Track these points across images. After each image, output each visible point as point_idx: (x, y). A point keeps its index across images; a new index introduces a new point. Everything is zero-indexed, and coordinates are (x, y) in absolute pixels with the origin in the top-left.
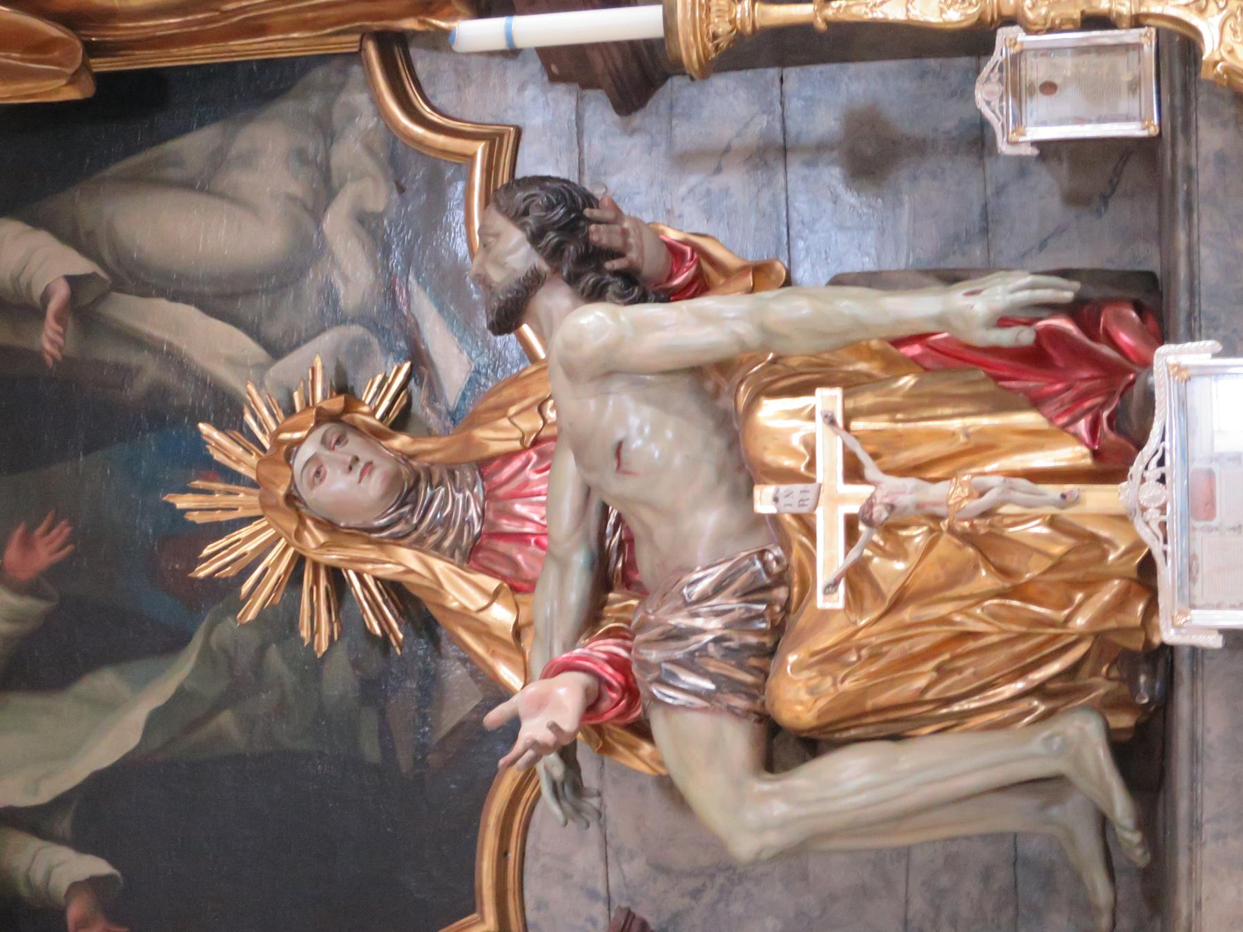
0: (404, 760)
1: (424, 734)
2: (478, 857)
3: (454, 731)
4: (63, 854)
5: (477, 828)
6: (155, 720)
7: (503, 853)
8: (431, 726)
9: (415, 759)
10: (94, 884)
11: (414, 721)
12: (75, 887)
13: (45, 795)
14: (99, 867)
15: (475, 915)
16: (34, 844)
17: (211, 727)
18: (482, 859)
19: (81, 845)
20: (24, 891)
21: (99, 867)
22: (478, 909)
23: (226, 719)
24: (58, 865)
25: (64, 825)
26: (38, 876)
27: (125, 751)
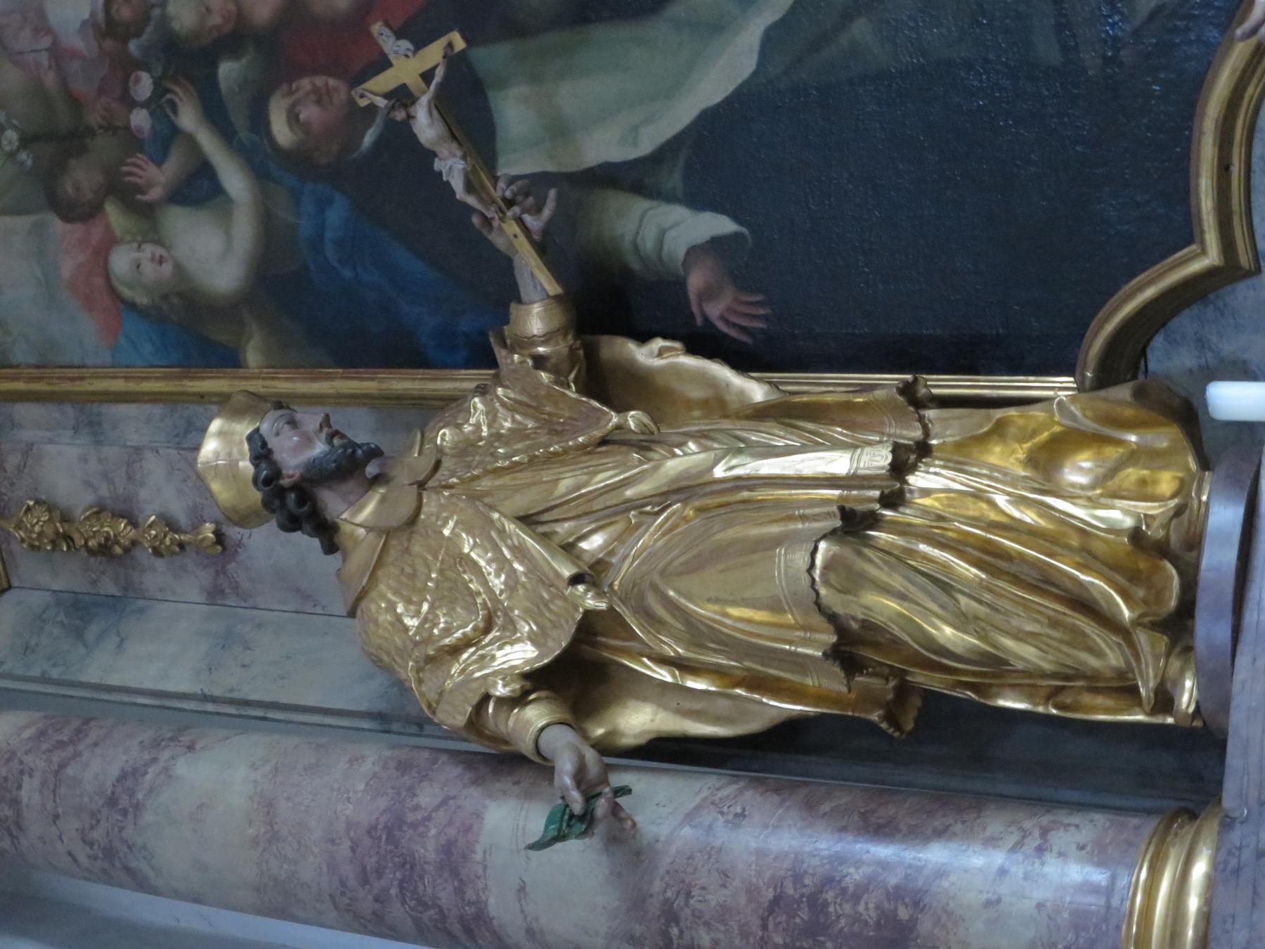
0: (1090, 58)
1: (1113, 26)
2: (1192, 170)
3: (1153, 16)
4: (676, 213)
5: (1189, 140)
6: (772, 39)
7: (1224, 168)
8: (1122, 14)
9: (1105, 58)
10: (717, 245)
11: (1100, 9)
12: (695, 252)
13: (646, 146)
14: (723, 225)
15: (1193, 247)
16: (640, 205)
17: (844, 39)
18: (1198, 175)
19: (697, 201)
20: (636, 266)
21: (723, 225)
22: (1197, 239)
23: (861, 29)
24: (671, 227)
25: (674, 179)
26: (648, 245)
27: (740, 81)
